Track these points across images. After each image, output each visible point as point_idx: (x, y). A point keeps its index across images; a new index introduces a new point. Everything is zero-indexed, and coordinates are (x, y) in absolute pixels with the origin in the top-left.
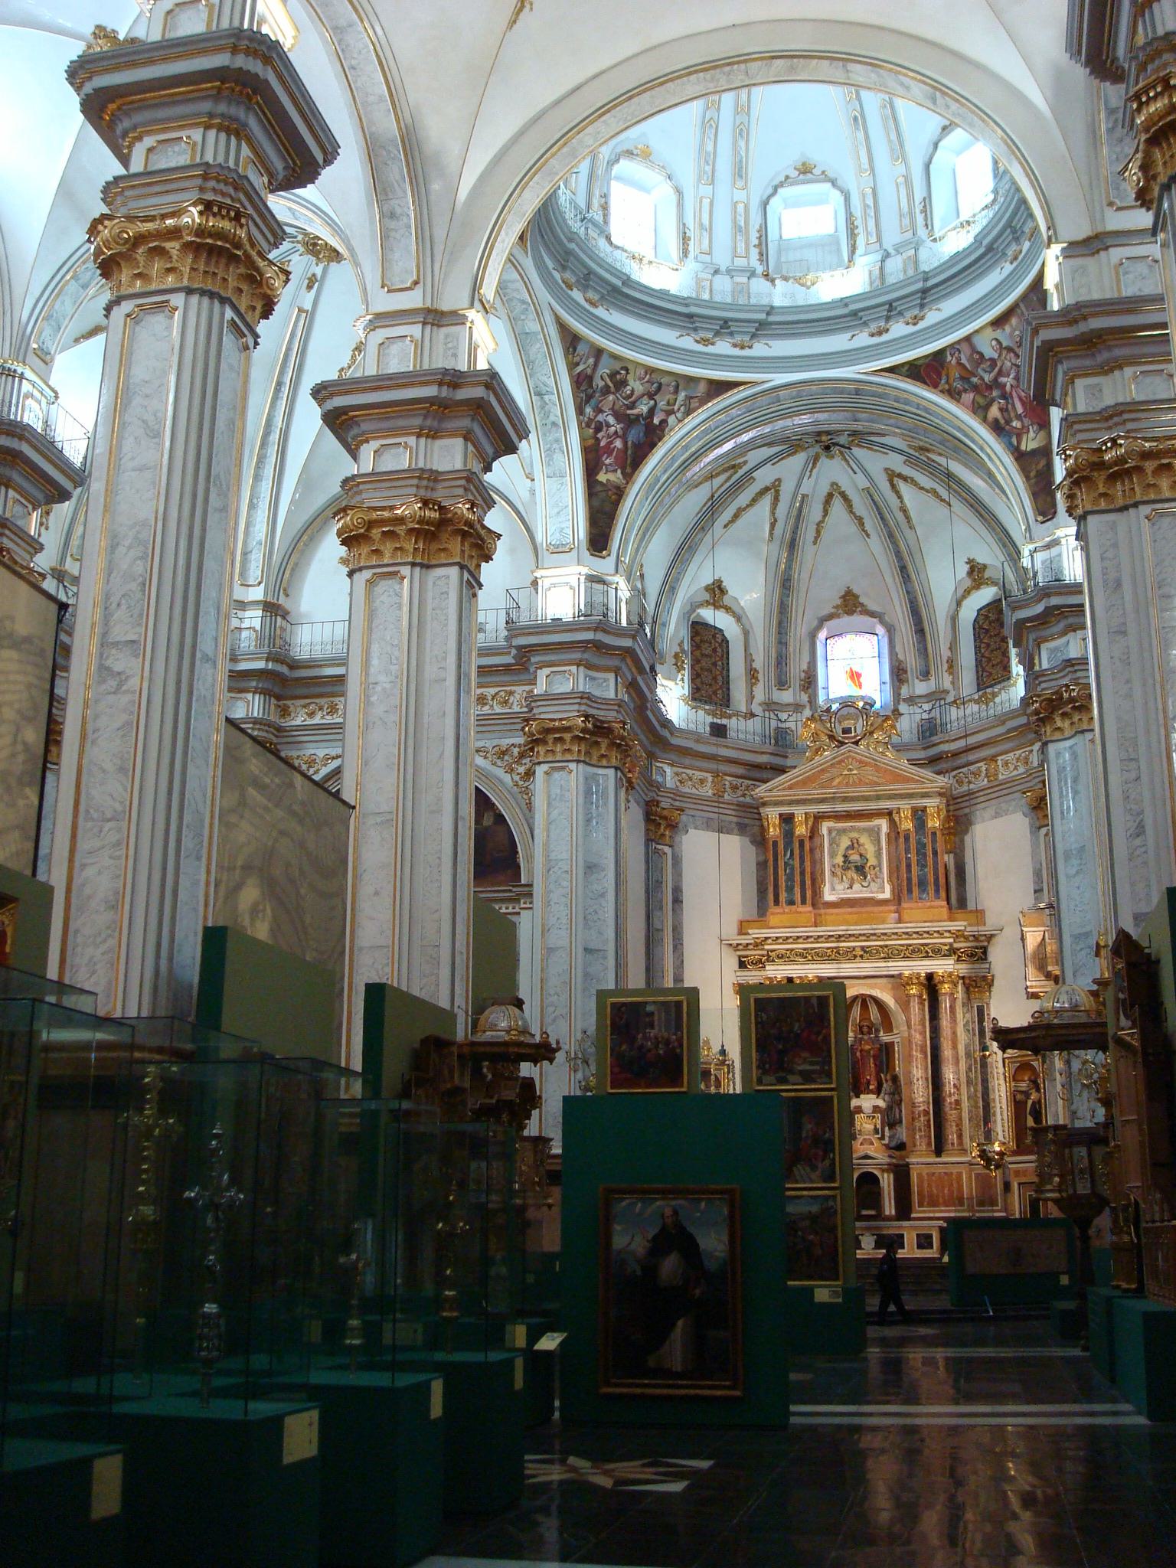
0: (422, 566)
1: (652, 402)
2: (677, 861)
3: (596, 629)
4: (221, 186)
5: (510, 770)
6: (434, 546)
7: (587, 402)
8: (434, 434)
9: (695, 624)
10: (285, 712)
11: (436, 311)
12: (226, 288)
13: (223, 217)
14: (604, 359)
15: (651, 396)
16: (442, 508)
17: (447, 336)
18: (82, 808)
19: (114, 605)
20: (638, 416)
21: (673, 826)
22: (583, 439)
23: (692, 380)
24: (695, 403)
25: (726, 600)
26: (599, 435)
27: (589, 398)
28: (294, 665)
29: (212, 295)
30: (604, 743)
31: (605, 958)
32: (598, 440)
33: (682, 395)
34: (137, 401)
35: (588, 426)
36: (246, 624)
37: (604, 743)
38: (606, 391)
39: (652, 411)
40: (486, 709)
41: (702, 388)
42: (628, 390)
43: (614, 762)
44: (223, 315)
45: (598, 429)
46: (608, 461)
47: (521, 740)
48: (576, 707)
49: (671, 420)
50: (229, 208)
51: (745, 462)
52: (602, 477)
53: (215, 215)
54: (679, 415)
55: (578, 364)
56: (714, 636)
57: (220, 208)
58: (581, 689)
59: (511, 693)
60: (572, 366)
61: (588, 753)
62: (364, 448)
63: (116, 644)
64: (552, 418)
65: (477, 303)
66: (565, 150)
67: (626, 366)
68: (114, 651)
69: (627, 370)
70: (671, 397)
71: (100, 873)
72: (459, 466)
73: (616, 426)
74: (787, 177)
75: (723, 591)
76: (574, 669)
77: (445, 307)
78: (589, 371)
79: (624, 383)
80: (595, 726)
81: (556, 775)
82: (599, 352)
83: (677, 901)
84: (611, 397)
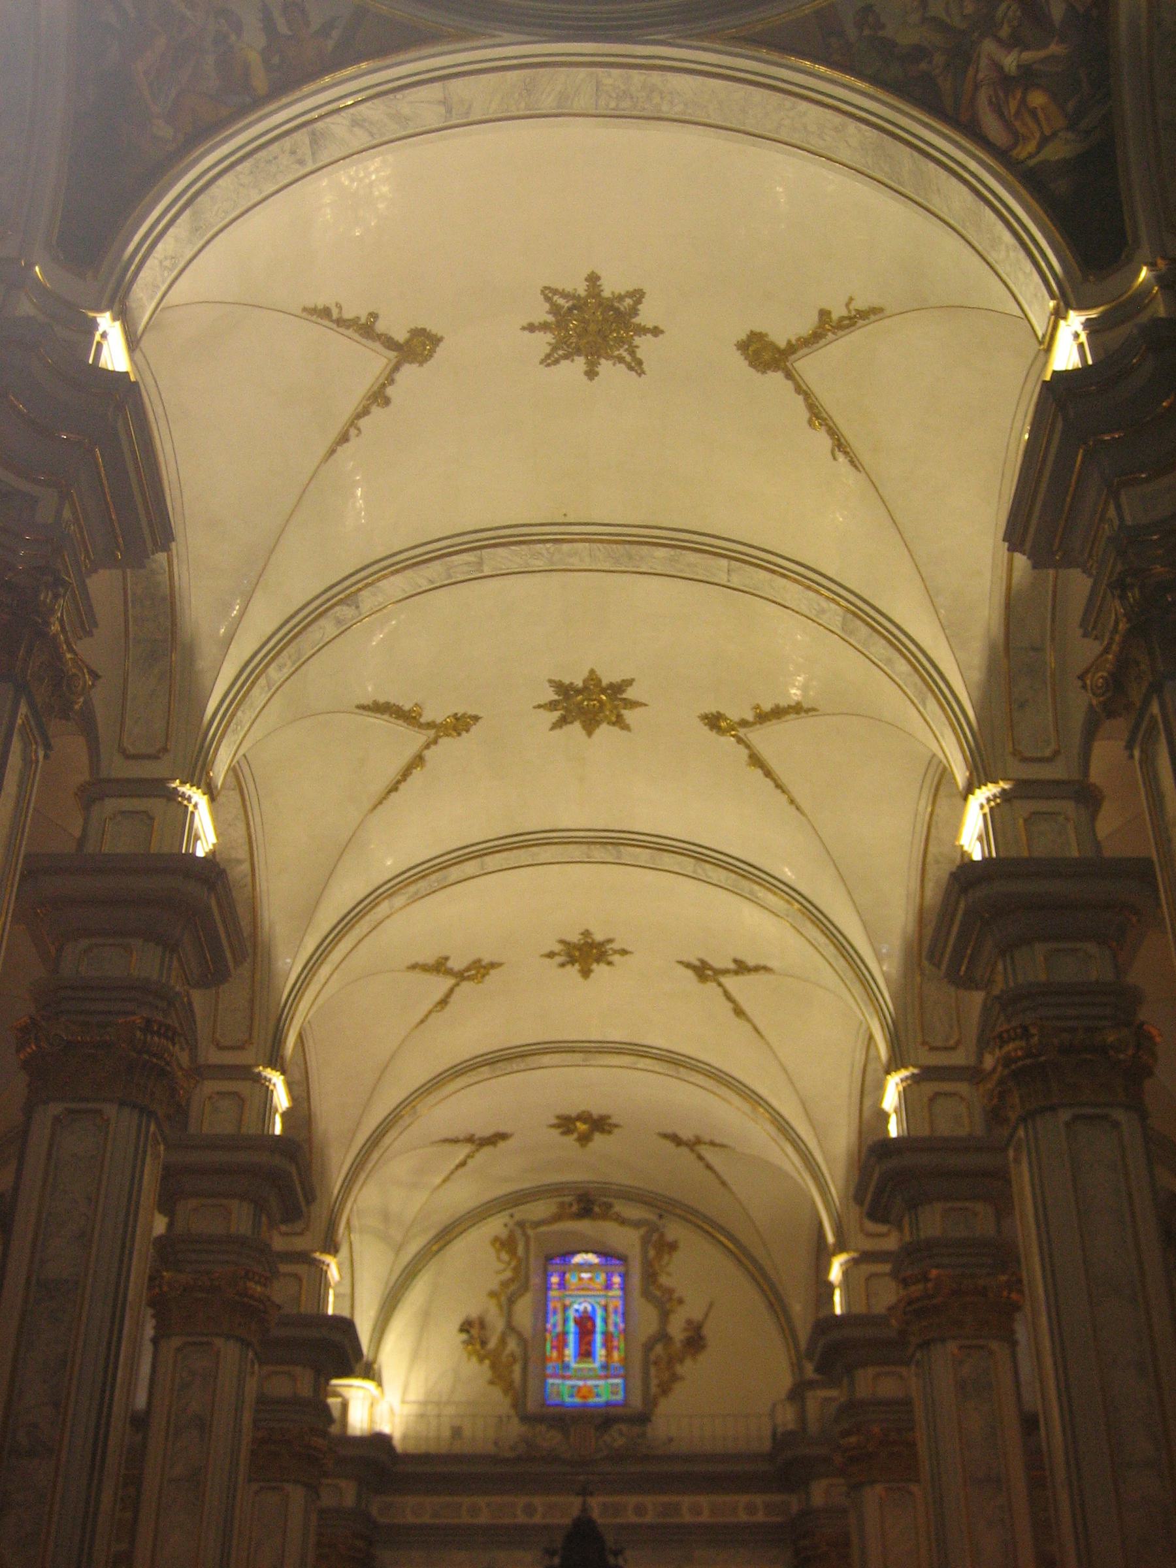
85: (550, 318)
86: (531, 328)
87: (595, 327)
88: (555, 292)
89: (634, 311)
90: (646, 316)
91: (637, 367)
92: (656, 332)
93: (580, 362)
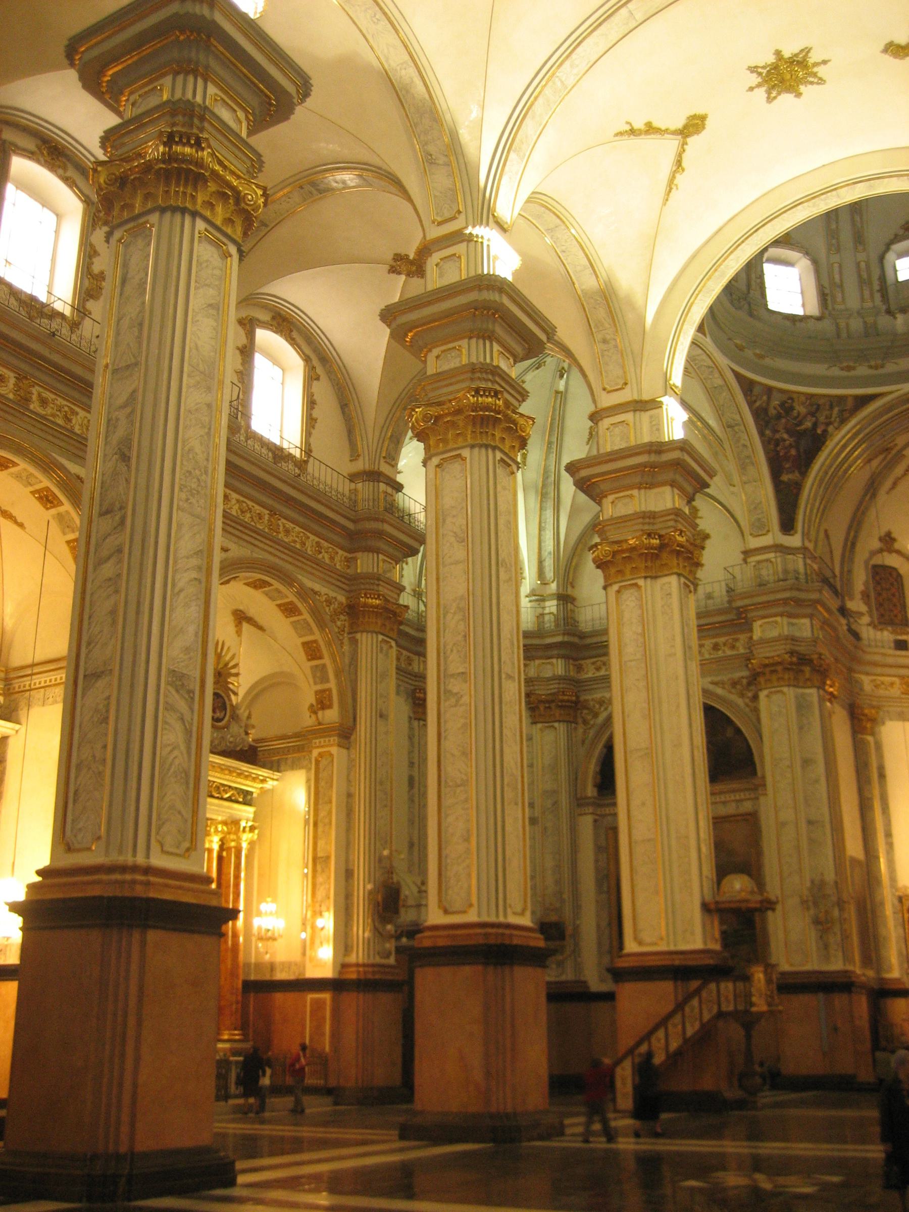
0: (652, 577)
1: (814, 419)
2: (879, 747)
3: (791, 589)
4: (484, 376)
5: (742, 695)
6: (658, 563)
7: (766, 426)
8: (651, 486)
9: (875, 567)
10: (579, 668)
11: (641, 401)
12: (494, 440)
13: (487, 396)
14: (775, 393)
15: (813, 414)
16: (660, 537)
17: (651, 417)
18: (443, 779)
19: (449, 652)
20: (805, 430)
21: (874, 721)
22: (767, 453)
23: (841, 399)
24: (846, 415)
25: (896, 546)
26: (778, 449)
27: (767, 423)
28: (582, 636)
29: (487, 446)
30: (807, 669)
31: (823, 826)
32: (778, 452)
33: (836, 410)
34: (449, 520)
35: (769, 442)
36: (547, 611)
37: (807, 669)
38: (779, 417)
39: (815, 425)
40: (720, 653)
41: (850, 403)
42: (795, 413)
43: (817, 684)
44: (494, 457)
45: (777, 445)
46: (787, 466)
47: (745, 673)
48: (783, 647)
49: (831, 429)
50: (490, 390)
51: (896, 445)
52: (785, 478)
53: (481, 396)
54: (836, 425)
55: (755, 401)
56: (891, 574)
57: (484, 391)
58: (786, 633)
59: (737, 640)
60: (750, 404)
61: (796, 679)
62: (604, 500)
63: (452, 676)
64: (742, 442)
65: (669, 390)
66: (717, 274)
67: (790, 396)
68: (452, 680)
69: (792, 399)
70: (828, 413)
71: (457, 818)
72: (669, 505)
73: (789, 440)
74: (896, 236)
75: (894, 540)
76: (778, 619)
77: (645, 397)
78: (764, 405)
79: (792, 408)
80: (799, 659)
81: (774, 697)
82: (769, 390)
83: (882, 776)
84: (783, 420)
85: (815, 70)
86: (825, 62)
87: (786, 74)
88: (818, 84)
89: (769, 93)
90: (761, 93)
91: (753, 69)
92: (751, 89)
93: (787, 54)
